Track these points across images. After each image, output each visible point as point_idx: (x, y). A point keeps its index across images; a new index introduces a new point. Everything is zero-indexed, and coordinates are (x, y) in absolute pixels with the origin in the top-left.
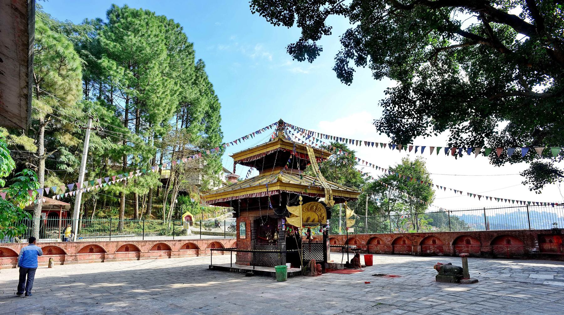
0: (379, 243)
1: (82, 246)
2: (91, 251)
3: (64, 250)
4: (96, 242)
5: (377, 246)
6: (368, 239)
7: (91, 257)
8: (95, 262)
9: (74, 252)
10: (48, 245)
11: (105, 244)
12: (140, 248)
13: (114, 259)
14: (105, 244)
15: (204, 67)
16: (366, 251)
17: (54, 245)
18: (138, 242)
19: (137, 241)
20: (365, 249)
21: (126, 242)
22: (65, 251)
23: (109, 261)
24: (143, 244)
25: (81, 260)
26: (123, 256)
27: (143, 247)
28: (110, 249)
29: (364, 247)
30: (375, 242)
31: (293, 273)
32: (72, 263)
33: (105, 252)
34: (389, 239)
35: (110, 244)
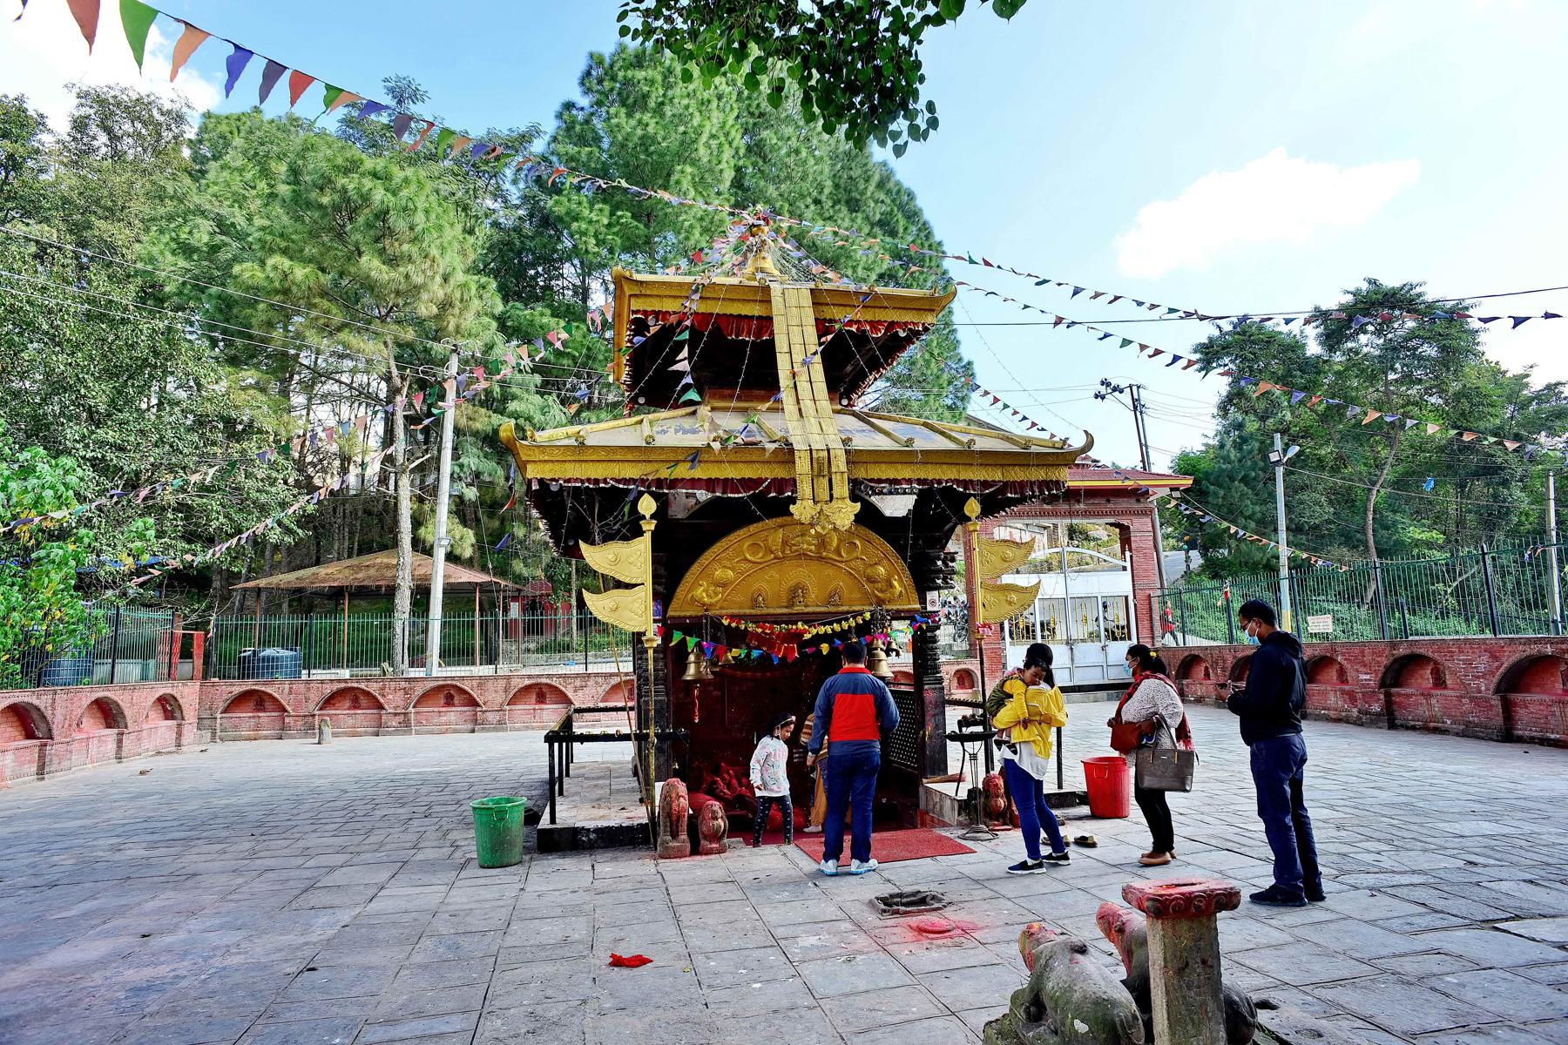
0: (1440, 683)
1: (419, 691)
4: (452, 678)
5: (1428, 696)
6: (1385, 661)
7: (444, 719)
8: (456, 731)
9: (401, 703)
10: (343, 685)
11: (475, 683)
12: (570, 695)
13: (500, 725)
14: (475, 683)
16: (1378, 715)
18: (565, 676)
19: (560, 676)
20: (1376, 708)
21: (529, 677)
23: (487, 730)
24: (578, 683)
26: (527, 718)
27: (580, 693)
28: (492, 697)
29: (1369, 696)
30: (1425, 677)
31: (598, 831)
32: (396, 732)
33: (478, 705)
34: (1482, 663)
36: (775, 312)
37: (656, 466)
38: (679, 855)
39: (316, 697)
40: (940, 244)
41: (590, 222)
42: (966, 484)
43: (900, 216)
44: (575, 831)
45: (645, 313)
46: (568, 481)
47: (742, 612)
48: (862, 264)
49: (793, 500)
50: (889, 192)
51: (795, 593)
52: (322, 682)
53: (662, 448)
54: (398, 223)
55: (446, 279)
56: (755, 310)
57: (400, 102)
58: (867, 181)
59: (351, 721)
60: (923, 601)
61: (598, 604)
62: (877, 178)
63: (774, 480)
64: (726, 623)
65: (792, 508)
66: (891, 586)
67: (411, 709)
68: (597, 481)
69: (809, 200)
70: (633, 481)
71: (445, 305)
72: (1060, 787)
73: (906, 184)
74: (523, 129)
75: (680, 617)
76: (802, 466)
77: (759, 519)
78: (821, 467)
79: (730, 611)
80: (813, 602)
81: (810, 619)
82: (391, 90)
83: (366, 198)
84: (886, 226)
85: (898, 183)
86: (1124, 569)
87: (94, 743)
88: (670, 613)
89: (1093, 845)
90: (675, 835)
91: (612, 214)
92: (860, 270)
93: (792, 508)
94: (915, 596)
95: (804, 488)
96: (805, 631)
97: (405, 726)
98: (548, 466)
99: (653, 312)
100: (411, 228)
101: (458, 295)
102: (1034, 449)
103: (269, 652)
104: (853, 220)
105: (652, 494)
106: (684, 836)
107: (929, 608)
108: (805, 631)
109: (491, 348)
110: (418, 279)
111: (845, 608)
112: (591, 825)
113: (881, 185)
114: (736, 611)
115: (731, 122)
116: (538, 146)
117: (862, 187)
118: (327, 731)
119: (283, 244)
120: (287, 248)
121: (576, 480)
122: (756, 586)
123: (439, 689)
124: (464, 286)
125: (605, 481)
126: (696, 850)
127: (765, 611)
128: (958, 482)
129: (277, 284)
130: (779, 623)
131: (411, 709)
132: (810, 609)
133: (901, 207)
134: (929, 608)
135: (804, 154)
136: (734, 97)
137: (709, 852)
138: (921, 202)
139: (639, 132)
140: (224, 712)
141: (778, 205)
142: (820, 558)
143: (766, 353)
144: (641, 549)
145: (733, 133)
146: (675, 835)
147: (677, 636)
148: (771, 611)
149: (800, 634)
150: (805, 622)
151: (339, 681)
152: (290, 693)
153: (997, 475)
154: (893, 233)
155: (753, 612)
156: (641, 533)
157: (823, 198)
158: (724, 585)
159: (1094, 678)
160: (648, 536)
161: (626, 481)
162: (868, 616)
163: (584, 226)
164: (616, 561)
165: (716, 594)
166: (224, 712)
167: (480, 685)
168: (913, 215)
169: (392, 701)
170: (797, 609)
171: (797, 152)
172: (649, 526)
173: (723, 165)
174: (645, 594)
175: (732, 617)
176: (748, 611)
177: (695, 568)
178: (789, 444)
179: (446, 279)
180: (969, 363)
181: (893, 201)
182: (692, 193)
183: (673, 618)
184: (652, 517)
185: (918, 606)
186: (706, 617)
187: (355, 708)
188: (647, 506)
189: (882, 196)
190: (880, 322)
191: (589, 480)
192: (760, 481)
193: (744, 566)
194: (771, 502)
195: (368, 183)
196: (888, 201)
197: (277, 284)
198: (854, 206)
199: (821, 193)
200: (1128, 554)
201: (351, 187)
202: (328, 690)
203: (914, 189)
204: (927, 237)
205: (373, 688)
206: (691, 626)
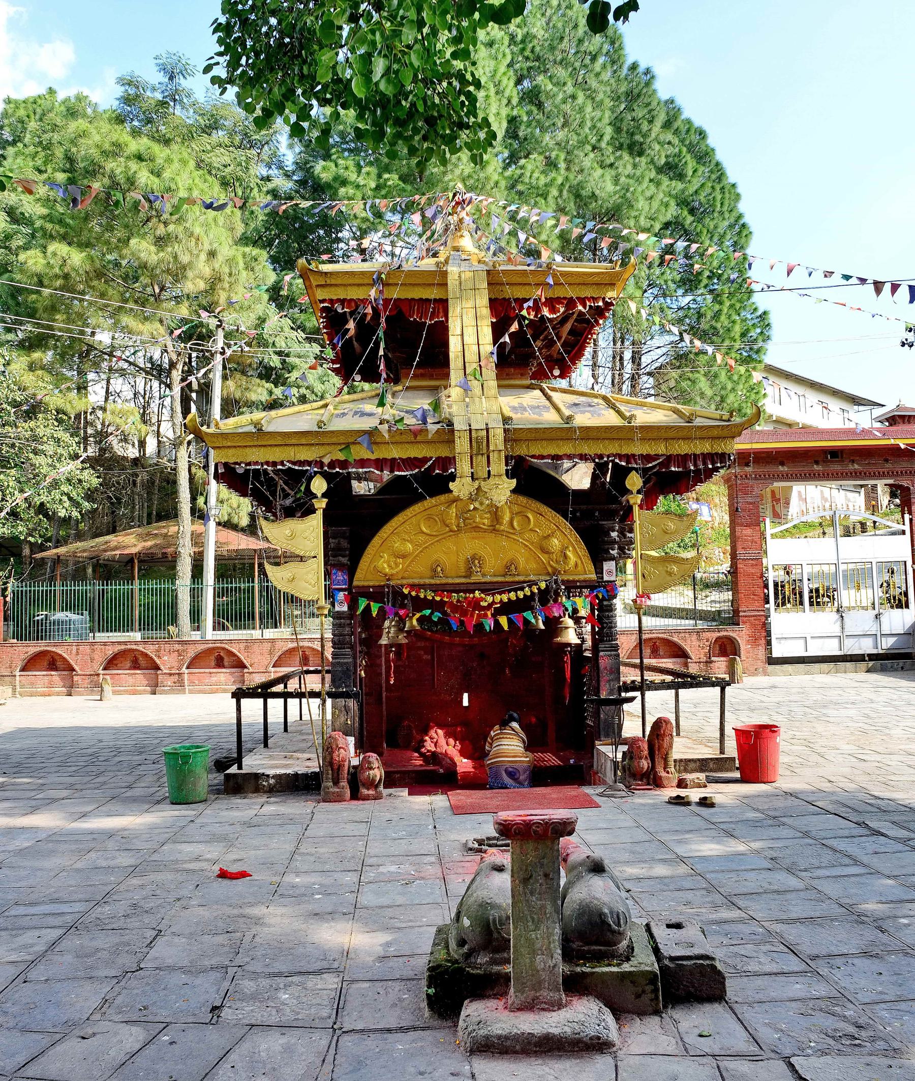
1: (192, 652)
2: (220, 663)
3: (156, 659)
4: (221, 641)
7: (214, 679)
9: (175, 664)
10: (123, 647)
11: (242, 646)
14: (242, 646)
15: (648, 84)
17: (134, 647)
22: (158, 661)
25: (192, 683)
31: (278, 777)
32: (172, 691)
33: (245, 667)
35: (256, 647)
36: (450, 296)
37: (328, 449)
38: (339, 799)
39: (100, 657)
40: (734, 185)
41: (358, 186)
42: (629, 458)
43: (688, 157)
44: (256, 776)
45: (331, 301)
46: (249, 464)
47: (422, 581)
48: (644, 213)
49: (453, 477)
50: (676, 132)
51: (473, 562)
52: (105, 644)
53: (333, 432)
55: (212, 254)
56: (433, 294)
57: (171, 78)
58: (650, 122)
59: (131, 680)
60: (599, 570)
61: (278, 576)
62: (661, 118)
63: (438, 459)
64: (406, 591)
65: (452, 485)
66: (565, 556)
67: (184, 670)
68: (274, 464)
69: (589, 148)
70: (309, 463)
71: (214, 282)
72: (722, 752)
73: (697, 122)
75: (363, 587)
76: (462, 445)
77: (421, 498)
78: (480, 445)
79: (410, 581)
80: (490, 571)
81: (488, 588)
82: (163, 68)
83: (131, 181)
84: (672, 169)
85: (689, 122)
86: (903, 532)
88: (355, 583)
89: (712, 805)
90: (336, 782)
91: (379, 176)
92: (642, 219)
93: (452, 485)
94: (590, 567)
95: (463, 467)
96: (482, 599)
97: (179, 685)
98: (231, 452)
99: (338, 300)
101: (227, 270)
102: (699, 422)
103: (60, 615)
104: (635, 166)
105: (325, 475)
106: (344, 783)
107: (606, 578)
108: (482, 599)
109: (264, 321)
110: (185, 259)
111: (521, 578)
112: (271, 772)
113: (667, 125)
114: (416, 581)
115: (502, 68)
117: (645, 126)
118: (108, 689)
119: (62, 231)
120: (66, 233)
121: (256, 463)
122: (435, 557)
123: (210, 651)
124: (230, 261)
125: (282, 463)
126: (355, 795)
127: (444, 581)
128: (621, 457)
129: (57, 270)
130: (457, 592)
131: (184, 670)
132: (488, 579)
133: (691, 148)
134: (606, 578)
135: (581, 98)
136: (506, 42)
138: (712, 141)
140: (23, 670)
141: (553, 155)
142: (494, 530)
143: (440, 334)
144: (314, 525)
145: (505, 81)
146: (336, 782)
147: (363, 603)
148: (450, 581)
150: (483, 591)
151: (119, 643)
152: (77, 653)
153: (661, 449)
154: (681, 177)
155: (433, 581)
156: (312, 510)
157: (603, 145)
158: (404, 557)
159: (866, 647)
160: (320, 513)
161: (300, 463)
162: (543, 585)
163: (351, 191)
164: (292, 536)
165: (397, 565)
166: (23, 670)
167: (247, 648)
168: (704, 156)
169: (167, 662)
170: (474, 579)
171: (574, 97)
172: (321, 504)
174: (317, 566)
175: (412, 586)
176: (427, 581)
177: (376, 541)
178: (450, 424)
179: (212, 254)
180: (765, 313)
181: (682, 141)
183: (358, 587)
184: (324, 495)
185: (593, 576)
186: (388, 586)
187: (135, 668)
188: (319, 486)
189: (669, 136)
190: (559, 300)
191: (267, 463)
192: (425, 460)
193: (421, 538)
194: (434, 480)
195: (134, 166)
196: (676, 141)
197: (57, 270)
198: (636, 149)
199: (599, 141)
200: (907, 517)
201: (118, 172)
202: (110, 651)
203: (706, 127)
205: (150, 650)
206: (376, 594)
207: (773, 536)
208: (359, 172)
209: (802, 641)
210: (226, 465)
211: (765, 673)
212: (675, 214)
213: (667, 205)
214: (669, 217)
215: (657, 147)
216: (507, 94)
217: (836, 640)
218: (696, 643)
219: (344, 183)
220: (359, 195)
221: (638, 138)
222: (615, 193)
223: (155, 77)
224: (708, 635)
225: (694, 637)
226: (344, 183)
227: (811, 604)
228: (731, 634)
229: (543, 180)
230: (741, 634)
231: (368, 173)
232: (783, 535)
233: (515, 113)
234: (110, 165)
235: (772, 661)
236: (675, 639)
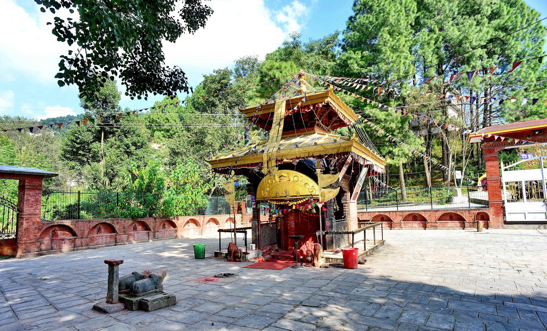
48: (474, 39)
54: (282, 81)
74: (333, 33)
87: (212, 229)
91: (362, 53)
100: (287, 81)
116: (341, 37)
126: (235, 261)
137: (237, 261)
139: (367, 21)
145: (410, 5)
149: (287, 205)
173: (402, 22)
177: (259, 187)
182: (389, 36)
204: (522, 12)
207: (506, 170)
208: (355, 53)
209: (523, 215)
210: (214, 169)
211: (503, 228)
212: (494, 34)
213: (488, 32)
214: (489, 37)
215: (487, 7)
216: (412, 9)
217: (544, 214)
218: (468, 215)
219: (351, 58)
220: (355, 62)
221: (476, 7)
222: (460, 35)
223: (291, 40)
224: (474, 211)
225: (467, 212)
226: (351, 58)
227: (528, 198)
228: (486, 212)
229: (427, 38)
230: (490, 212)
231: (358, 54)
232: (511, 169)
233: (418, 15)
234: (271, 73)
235: (506, 223)
236: (458, 213)
